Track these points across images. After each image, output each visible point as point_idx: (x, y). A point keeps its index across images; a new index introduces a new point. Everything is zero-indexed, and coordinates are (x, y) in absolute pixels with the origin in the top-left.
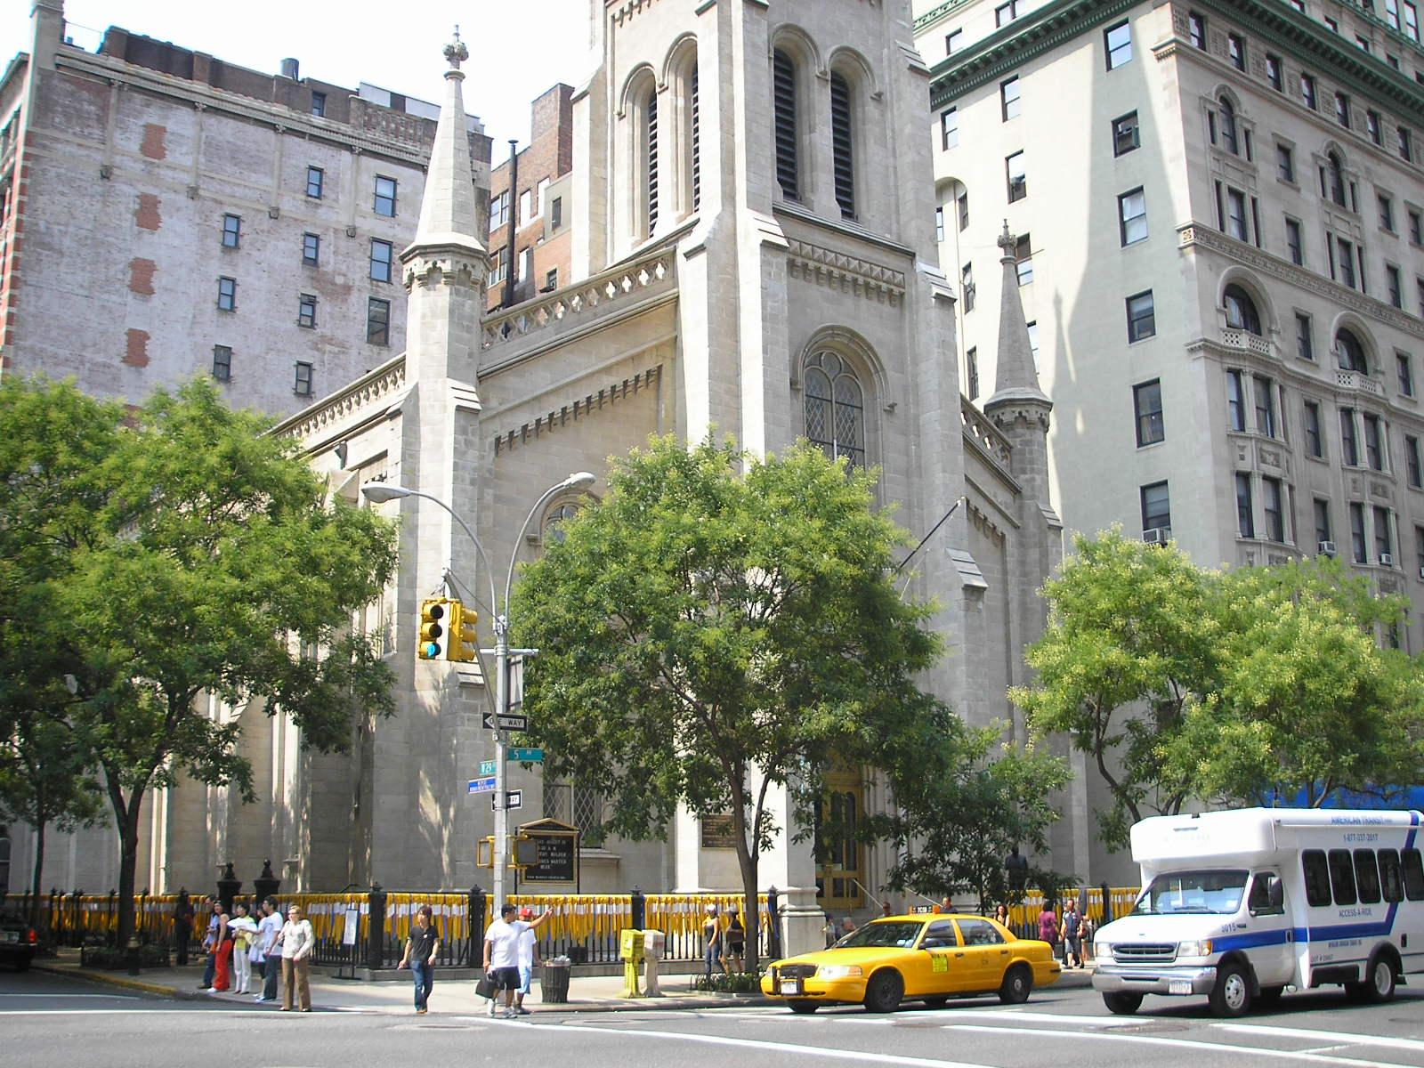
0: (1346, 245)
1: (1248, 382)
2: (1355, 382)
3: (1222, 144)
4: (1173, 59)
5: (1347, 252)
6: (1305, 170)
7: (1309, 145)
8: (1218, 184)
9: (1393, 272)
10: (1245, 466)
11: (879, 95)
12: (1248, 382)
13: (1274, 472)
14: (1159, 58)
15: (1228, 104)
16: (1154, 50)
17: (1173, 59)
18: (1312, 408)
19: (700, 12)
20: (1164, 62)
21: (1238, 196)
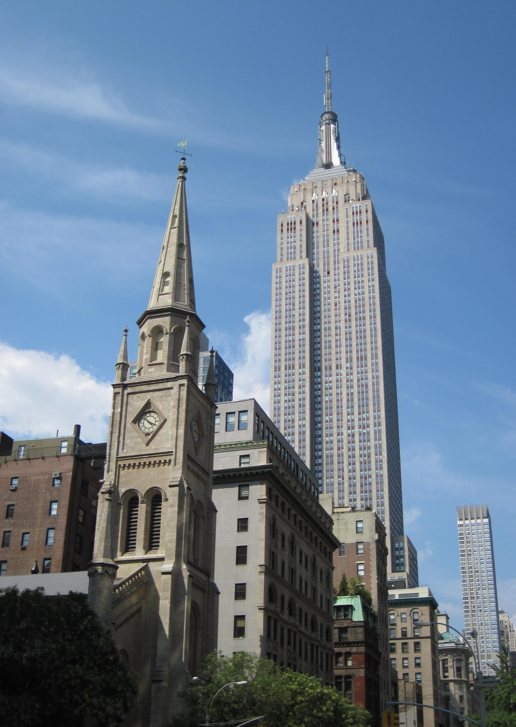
0: (292, 569)
1: (272, 621)
2: (292, 620)
3: (272, 536)
4: (264, 505)
5: (292, 571)
6: (287, 544)
7: (288, 534)
8: (270, 549)
9: (301, 579)
10: (269, 651)
11: (204, 517)
12: (272, 621)
13: (276, 653)
14: (260, 503)
15: (274, 519)
16: (258, 500)
17: (264, 505)
18: (282, 629)
19: (171, 486)
20: (261, 505)
21: (273, 553)
